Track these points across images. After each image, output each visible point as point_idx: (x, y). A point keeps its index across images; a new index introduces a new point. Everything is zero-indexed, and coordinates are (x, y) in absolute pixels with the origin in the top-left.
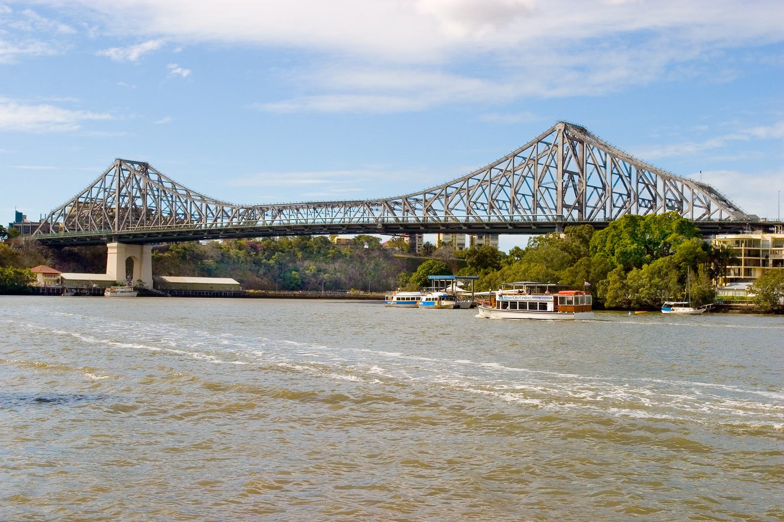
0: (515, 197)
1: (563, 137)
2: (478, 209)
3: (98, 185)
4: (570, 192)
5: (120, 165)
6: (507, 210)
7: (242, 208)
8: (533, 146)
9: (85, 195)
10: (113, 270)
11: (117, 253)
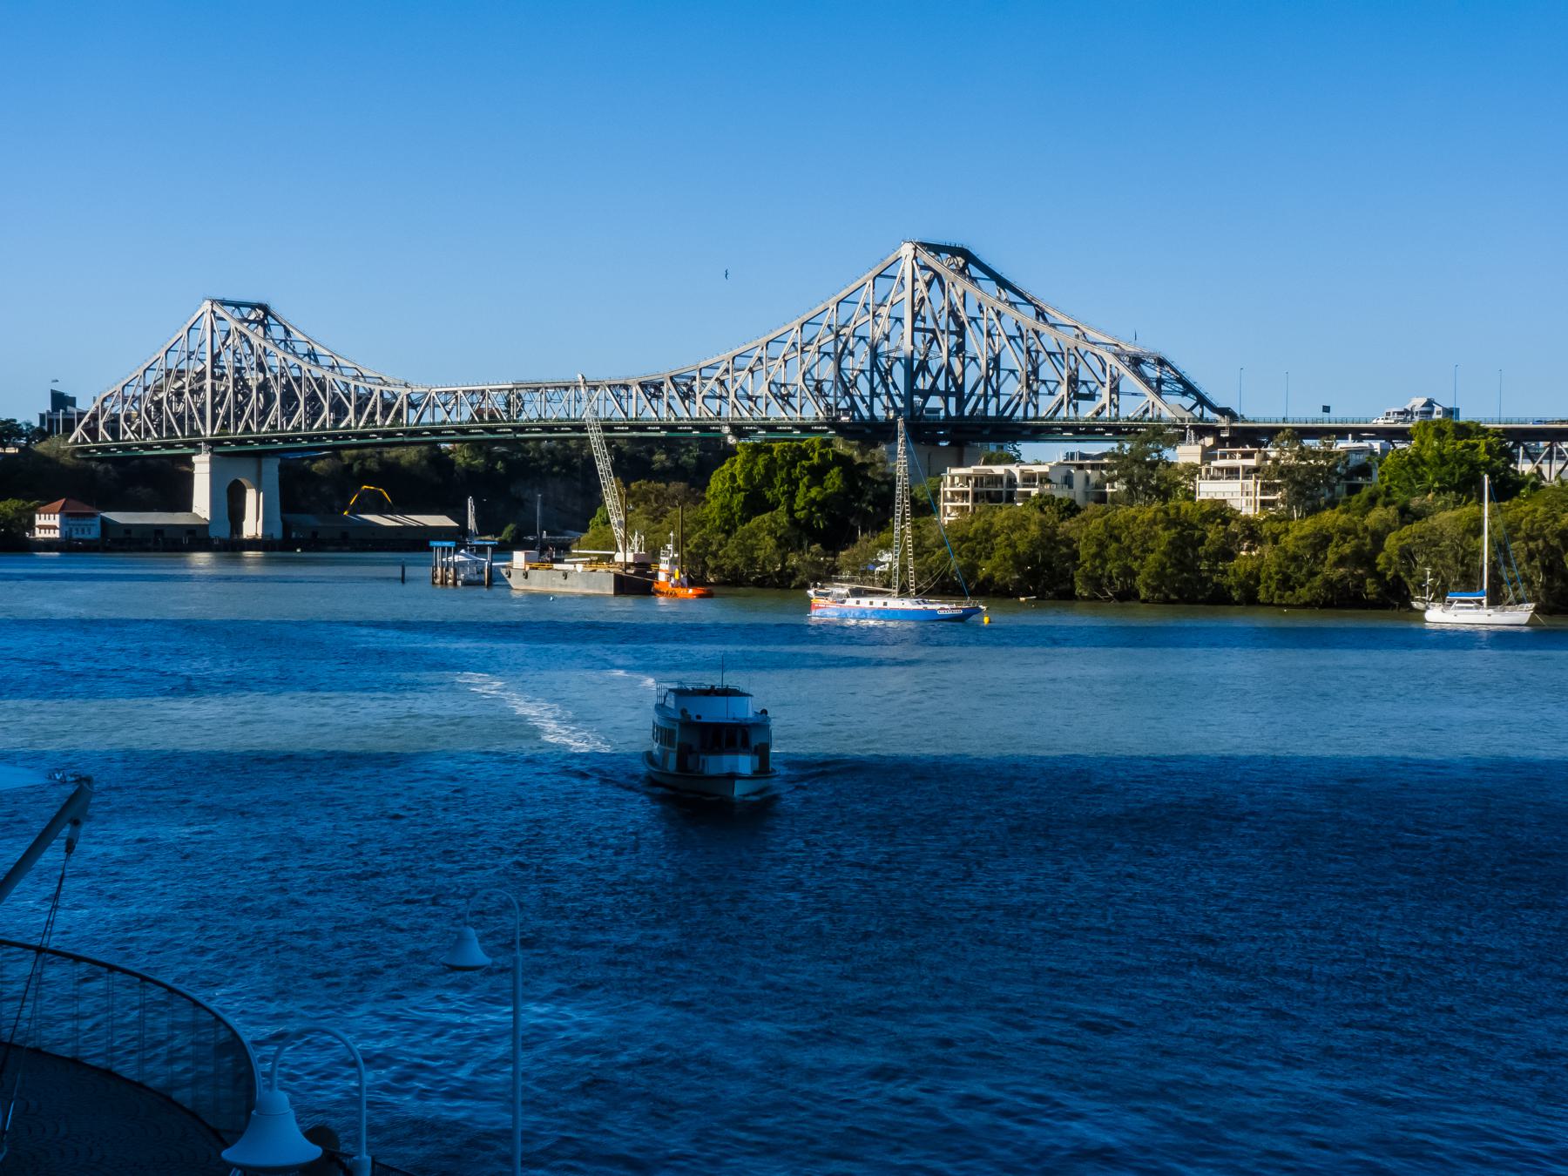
10: (202, 505)
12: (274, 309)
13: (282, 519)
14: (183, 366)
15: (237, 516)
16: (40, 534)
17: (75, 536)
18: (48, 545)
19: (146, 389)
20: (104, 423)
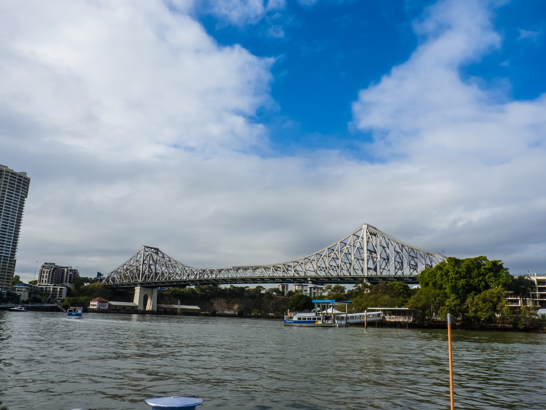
0: (341, 263)
1: (367, 232)
2: (321, 270)
3: (133, 259)
4: (371, 261)
5: (145, 249)
6: (336, 271)
7: (201, 270)
8: (351, 237)
9: (127, 264)
10: (136, 301)
11: (140, 292)
12: (160, 249)
13: (157, 305)
14: (134, 264)
15: (145, 304)
16: (91, 307)
17: (101, 308)
18: (93, 311)
19: (124, 270)
20: (111, 279)
